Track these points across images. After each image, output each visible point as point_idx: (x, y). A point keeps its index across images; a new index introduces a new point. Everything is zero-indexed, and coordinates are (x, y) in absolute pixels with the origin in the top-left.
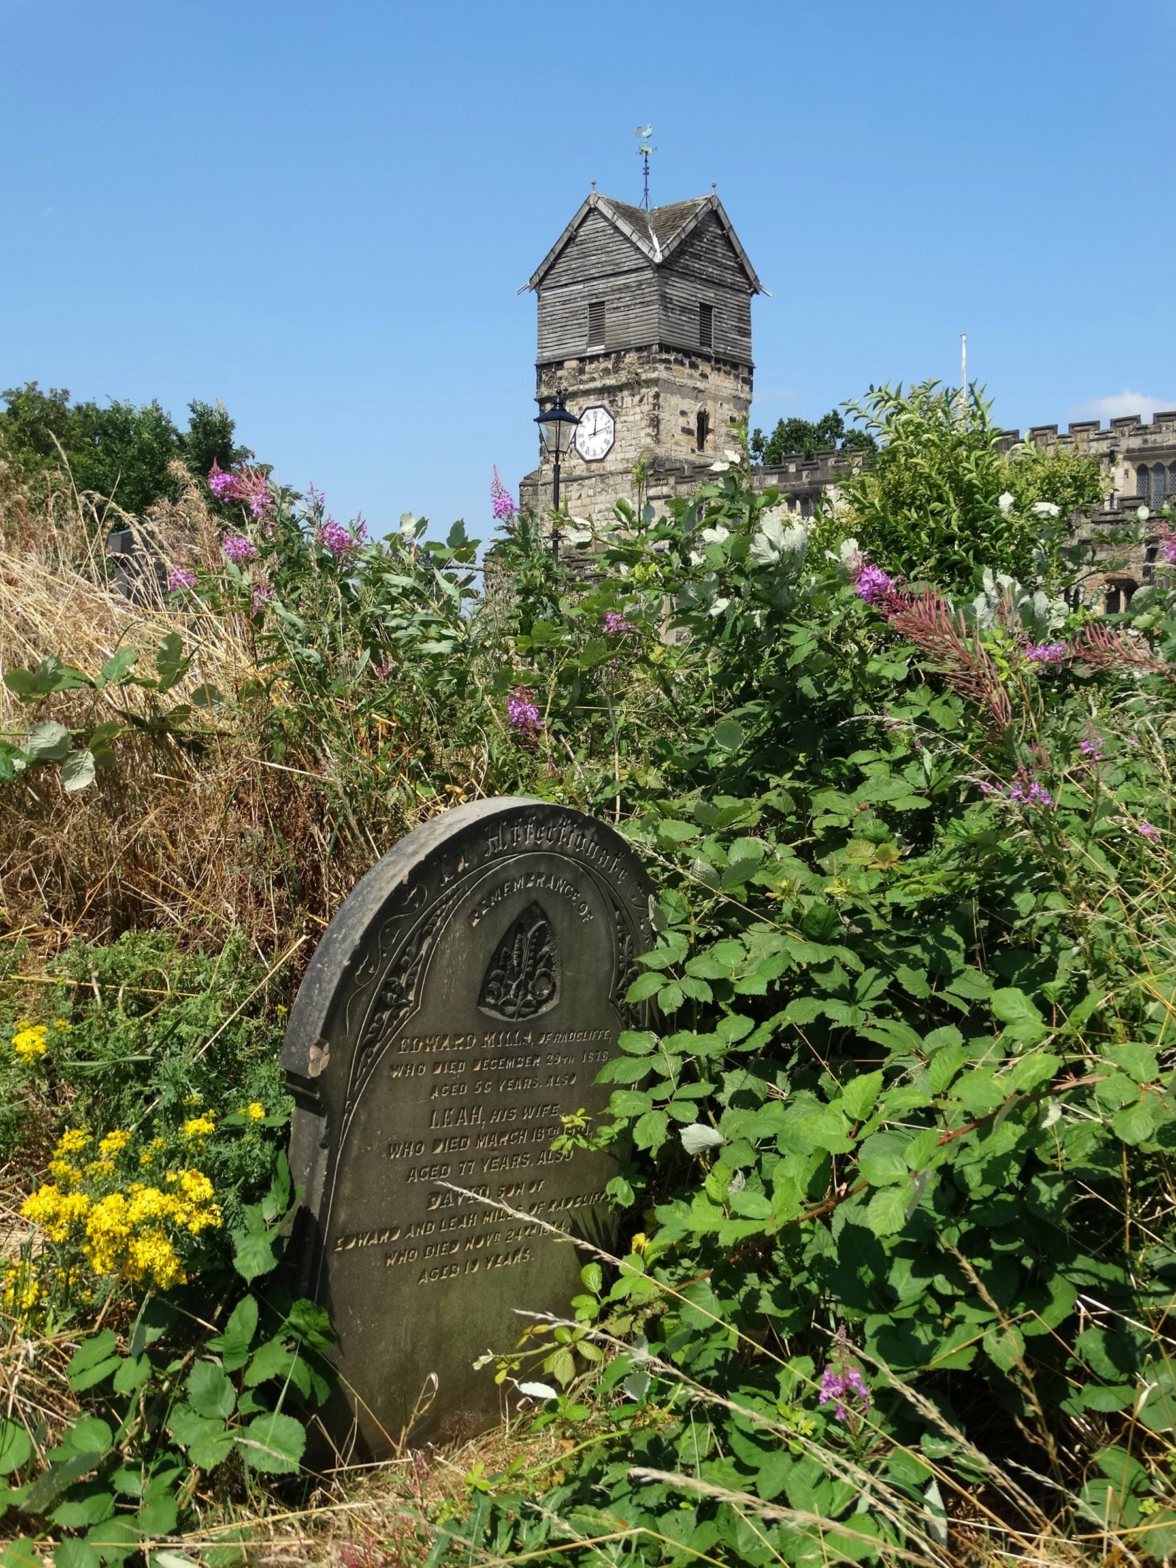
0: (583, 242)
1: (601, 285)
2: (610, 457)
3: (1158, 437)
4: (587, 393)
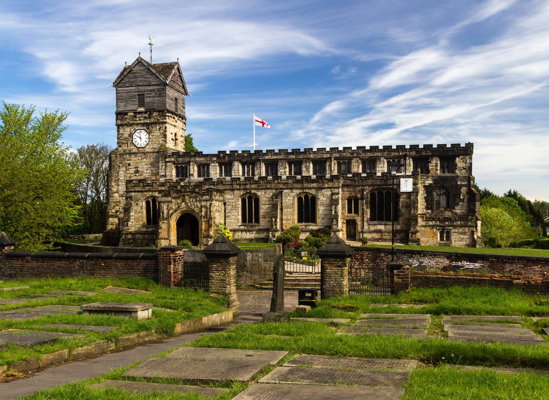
0: (135, 73)
1: (142, 88)
2: (147, 147)
3: (345, 154)
4: (137, 124)
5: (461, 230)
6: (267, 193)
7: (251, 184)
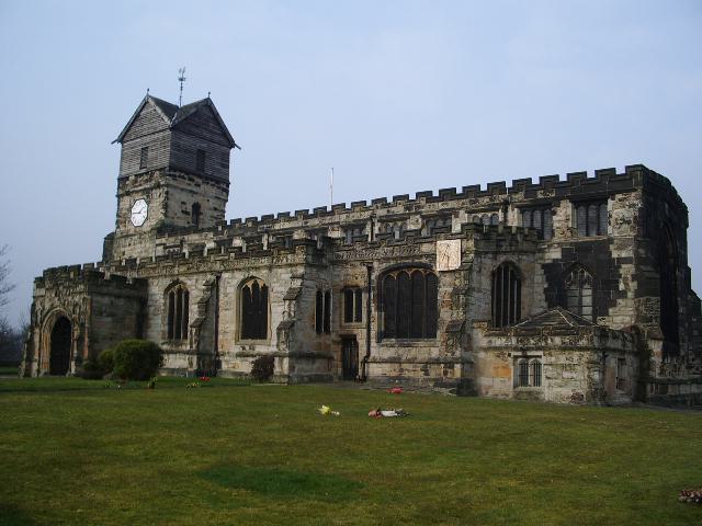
1: (147, 139)
4: (137, 192)
5: (562, 359)
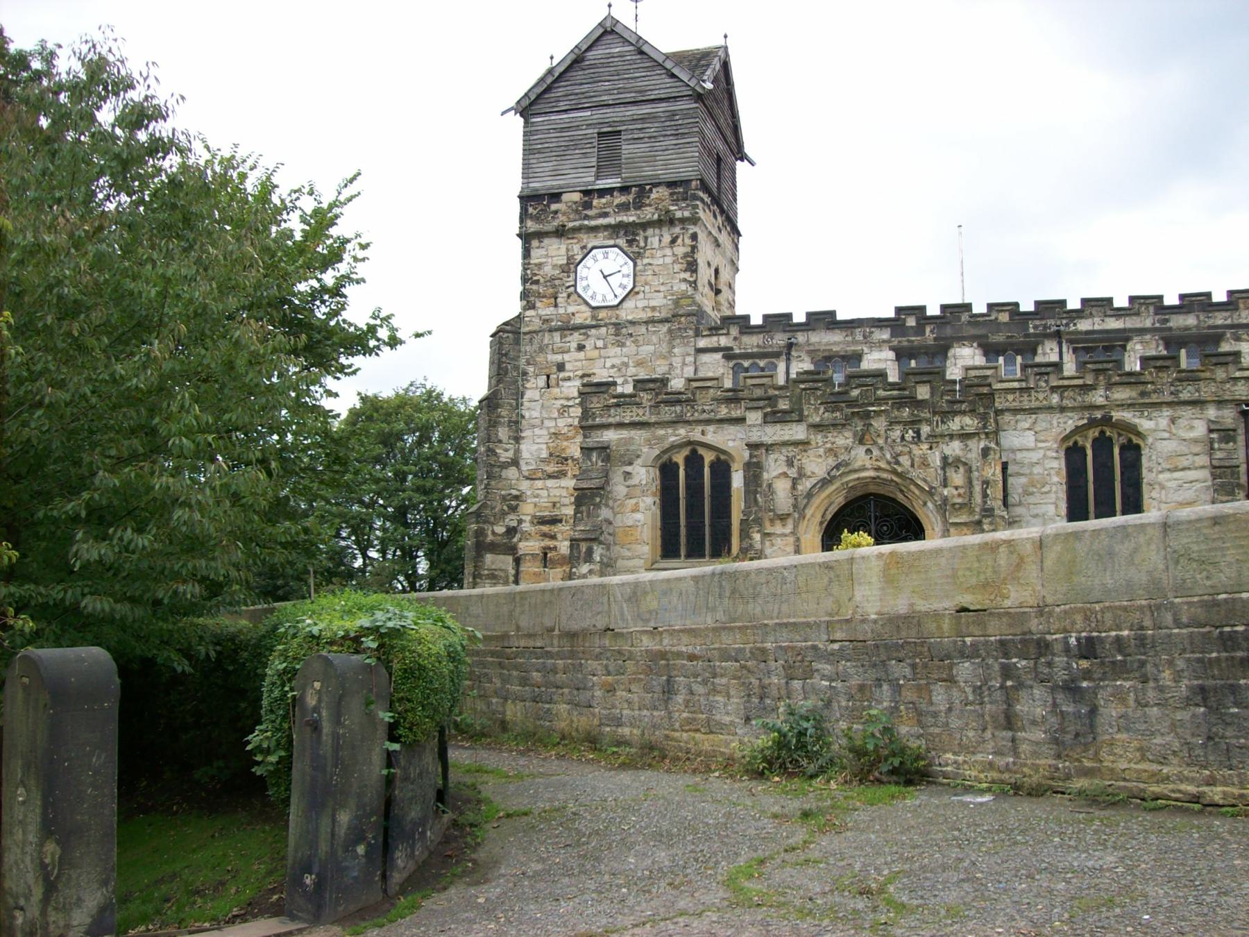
2: (625, 305)
6: (1182, 422)
7: (1110, 386)
